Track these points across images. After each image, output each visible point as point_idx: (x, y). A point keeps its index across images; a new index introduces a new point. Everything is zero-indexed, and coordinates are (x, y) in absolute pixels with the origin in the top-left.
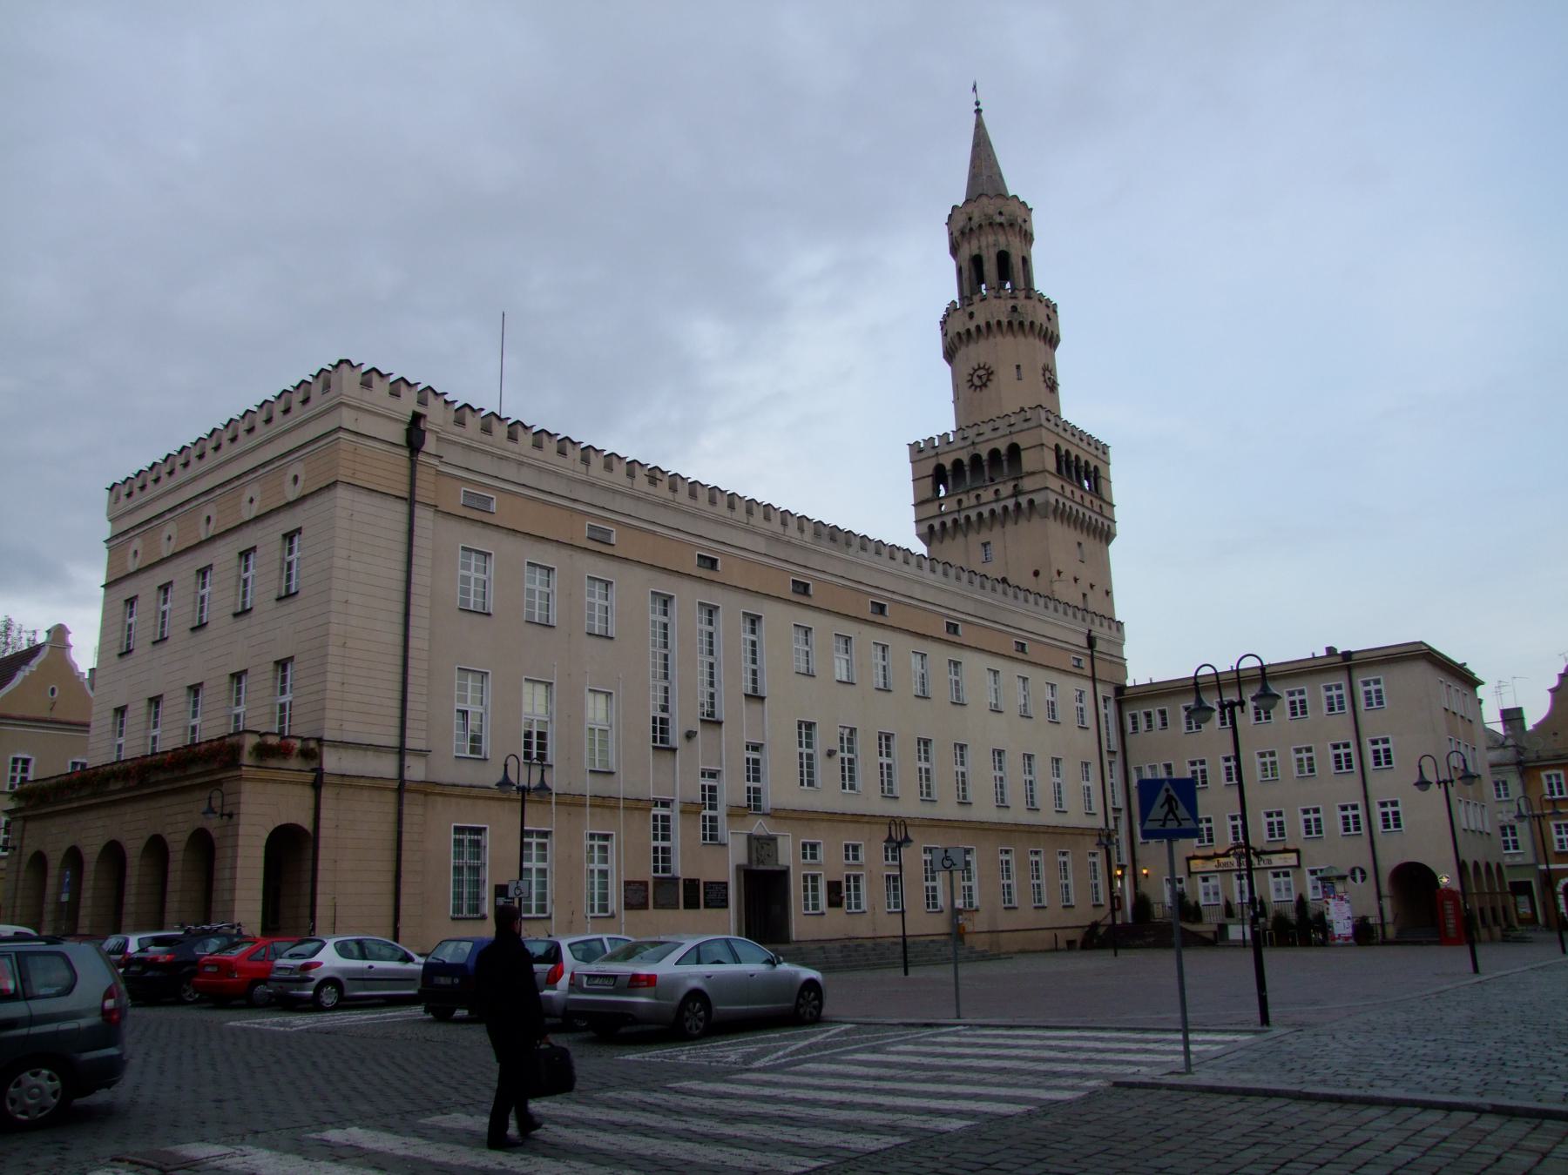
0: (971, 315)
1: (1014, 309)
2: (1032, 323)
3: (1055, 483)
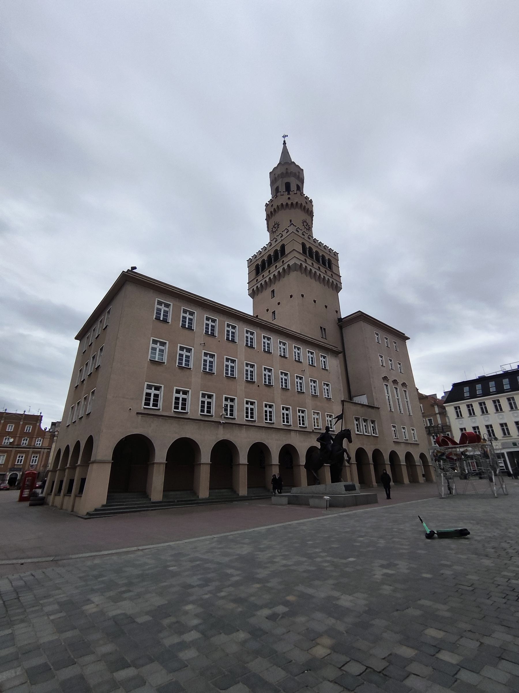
2: (297, 203)
3: (302, 258)
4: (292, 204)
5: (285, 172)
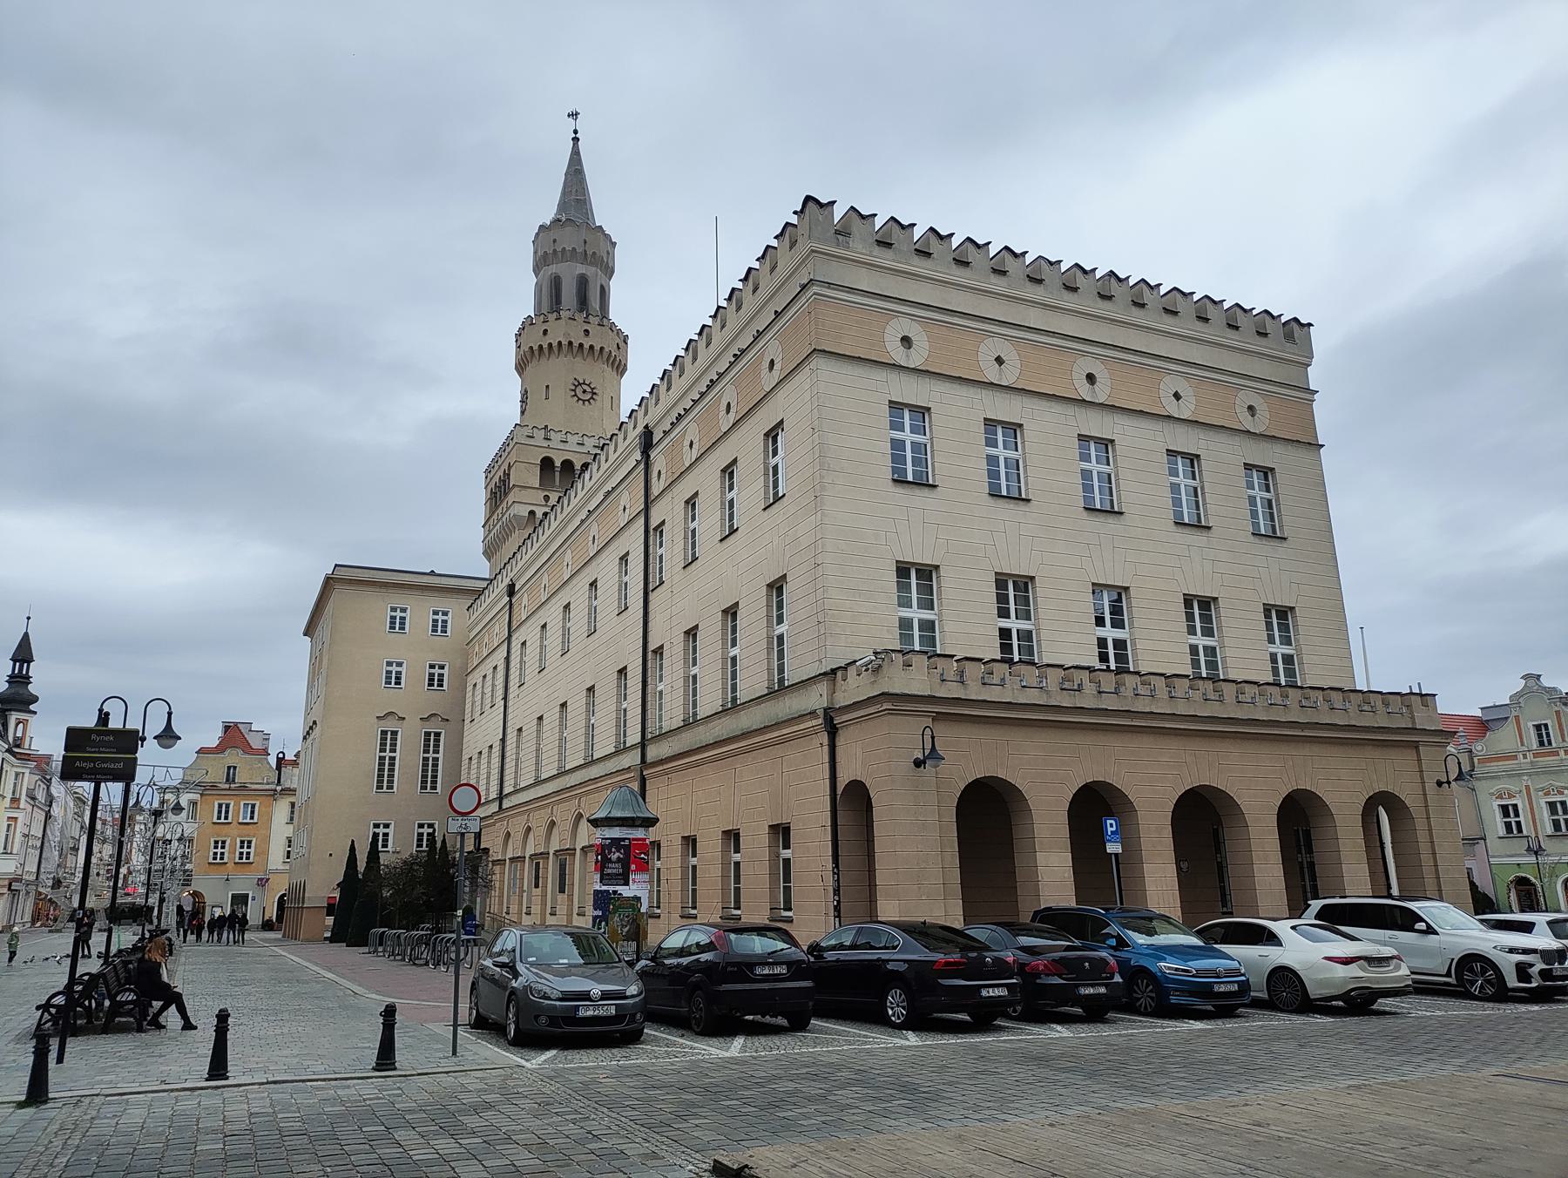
0: (545, 332)
1: (587, 332)
4: (591, 347)
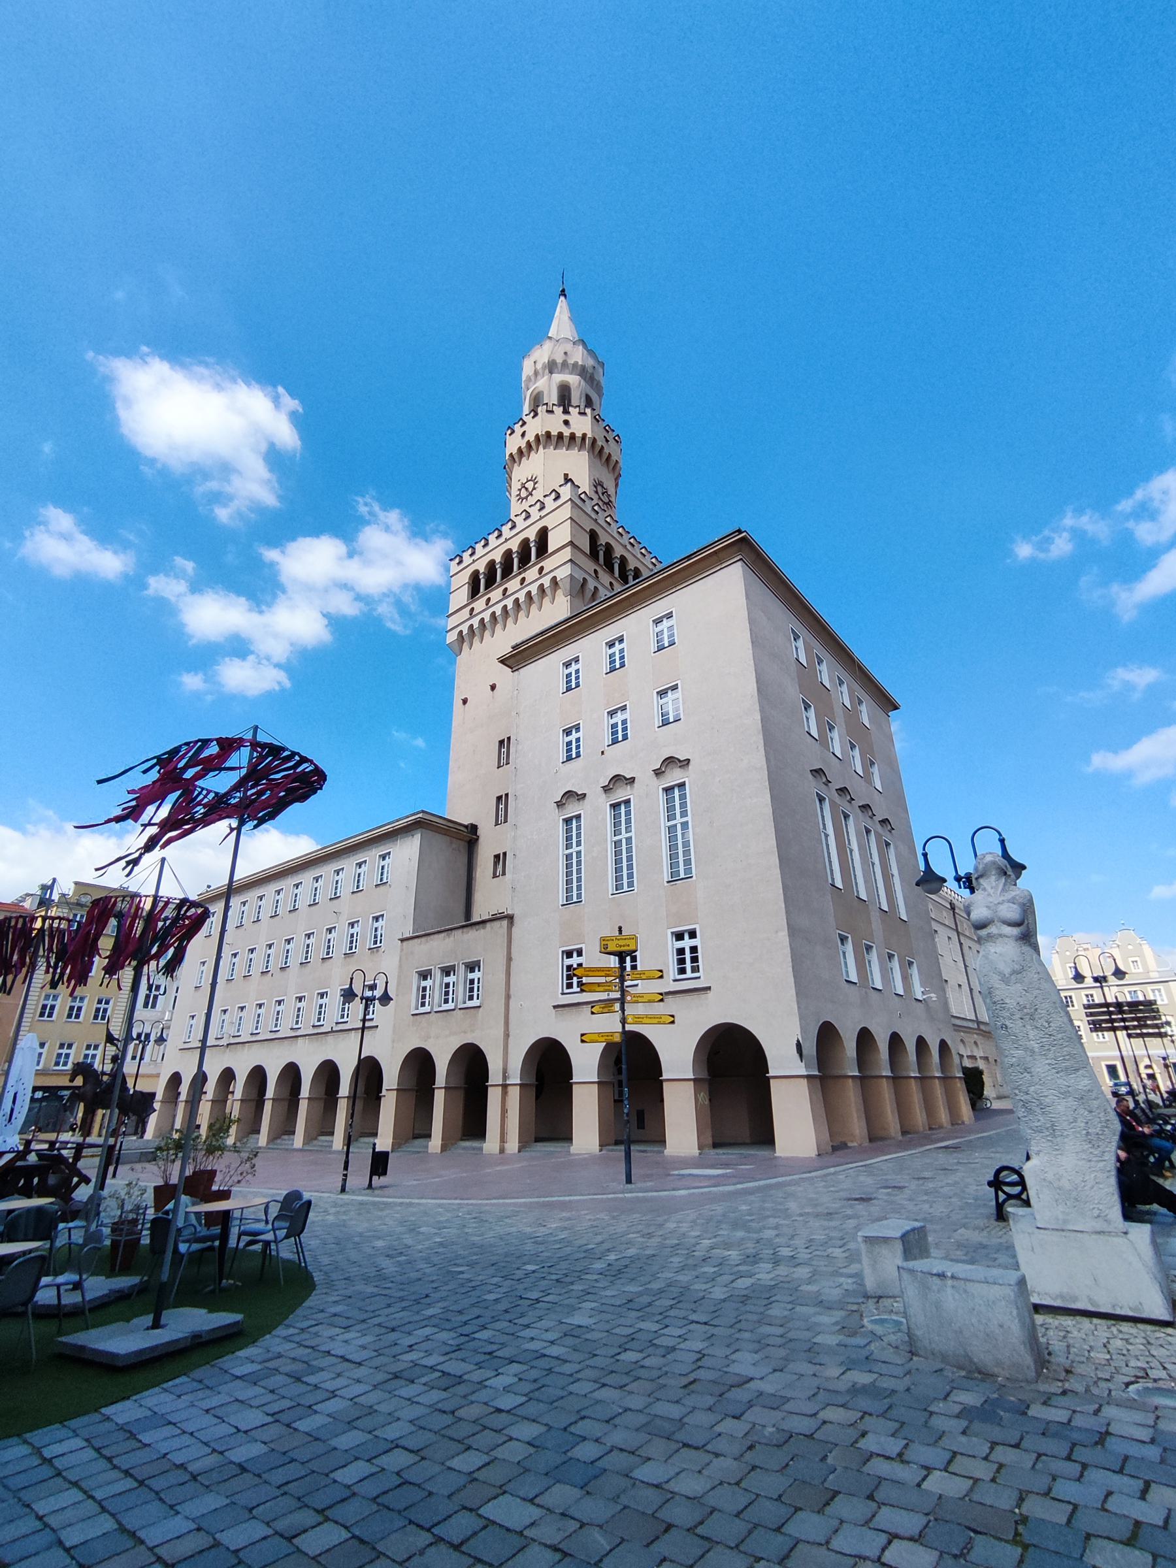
0: (523, 435)
1: (566, 423)
2: (584, 436)
3: (590, 566)
5: (559, 360)
